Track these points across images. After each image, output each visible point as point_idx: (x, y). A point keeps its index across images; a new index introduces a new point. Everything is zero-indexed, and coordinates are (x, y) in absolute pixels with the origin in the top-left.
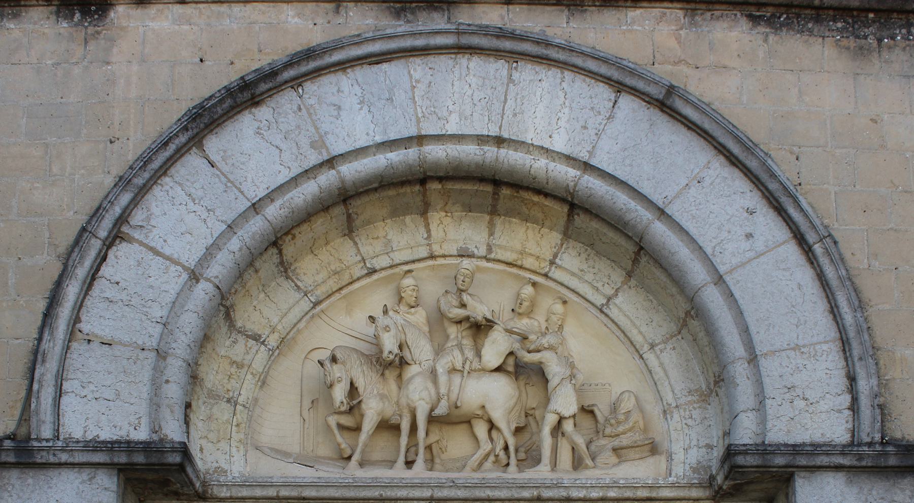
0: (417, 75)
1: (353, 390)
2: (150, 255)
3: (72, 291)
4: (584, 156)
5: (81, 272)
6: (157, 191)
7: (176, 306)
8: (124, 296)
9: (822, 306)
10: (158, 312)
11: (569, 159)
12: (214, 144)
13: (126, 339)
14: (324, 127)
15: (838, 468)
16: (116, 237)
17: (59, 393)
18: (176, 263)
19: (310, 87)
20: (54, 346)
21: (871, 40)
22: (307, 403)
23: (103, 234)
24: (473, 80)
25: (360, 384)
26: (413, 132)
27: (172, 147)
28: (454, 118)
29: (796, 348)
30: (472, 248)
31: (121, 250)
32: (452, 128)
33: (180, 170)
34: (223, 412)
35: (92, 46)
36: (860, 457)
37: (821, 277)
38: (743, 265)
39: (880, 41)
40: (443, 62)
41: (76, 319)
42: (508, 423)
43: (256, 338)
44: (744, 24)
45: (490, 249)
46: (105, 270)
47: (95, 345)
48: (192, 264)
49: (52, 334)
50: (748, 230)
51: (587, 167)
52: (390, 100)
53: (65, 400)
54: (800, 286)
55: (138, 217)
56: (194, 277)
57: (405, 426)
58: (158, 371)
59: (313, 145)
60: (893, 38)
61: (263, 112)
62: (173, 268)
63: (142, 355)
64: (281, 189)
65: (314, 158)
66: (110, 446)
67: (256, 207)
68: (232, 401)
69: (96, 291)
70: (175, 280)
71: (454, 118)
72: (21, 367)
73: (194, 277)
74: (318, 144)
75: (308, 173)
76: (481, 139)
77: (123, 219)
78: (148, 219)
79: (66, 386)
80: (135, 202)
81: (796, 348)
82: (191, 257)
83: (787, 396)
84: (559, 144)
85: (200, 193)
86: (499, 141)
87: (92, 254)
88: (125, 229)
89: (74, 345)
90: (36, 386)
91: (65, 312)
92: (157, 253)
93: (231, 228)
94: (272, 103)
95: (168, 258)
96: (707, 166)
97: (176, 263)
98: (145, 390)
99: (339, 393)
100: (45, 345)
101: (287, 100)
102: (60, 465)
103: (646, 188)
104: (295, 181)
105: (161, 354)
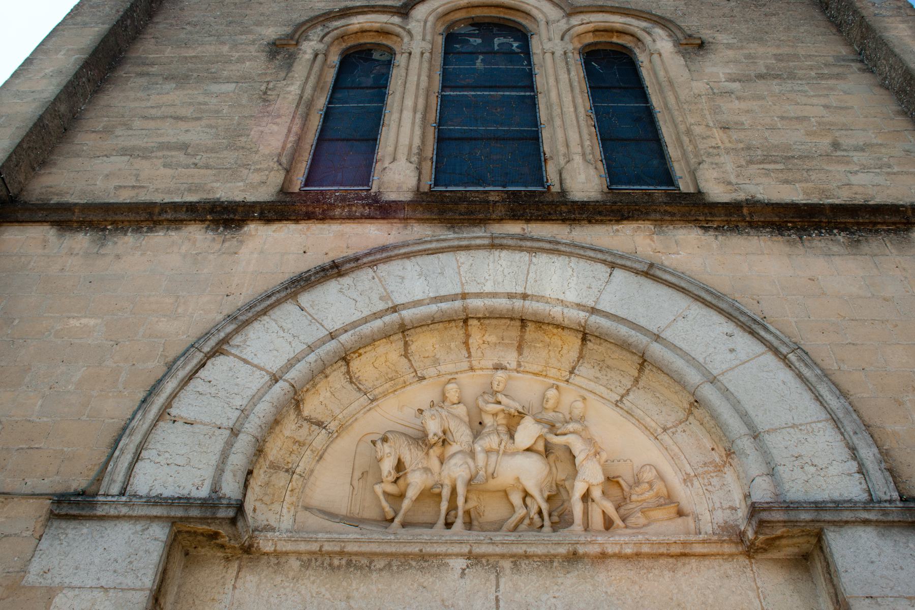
0: (461, 260)
1: (400, 466)
3: (170, 386)
5: (182, 374)
6: (256, 325)
7: (256, 399)
8: (213, 390)
9: (807, 396)
10: (238, 402)
11: (579, 306)
12: (305, 299)
13: (206, 419)
14: (390, 289)
15: (866, 522)
16: (218, 351)
17: (137, 458)
18: (261, 369)
19: (382, 267)
20: (142, 425)
22: (357, 474)
23: (206, 349)
24: (504, 263)
25: (407, 459)
26: (458, 290)
27: (274, 298)
29: (794, 426)
30: (505, 363)
31: (220, 360)
32: (488, 288)
33: (277, 313)
34: (281, 479)
35: (227, 244)
36: (885, 512)
37: (800, 376)
38: (732, 369)
40: (481, 254)
41: (168, 404)
42: (541, 491)
43: (320, 424)
45: (519, 365)
46: (202, 373)
47: (179, 424)
49: (144, 415)
50: (731, 347)
52: (442, 273)
53: (140, 465)
54: (784, 383)
55: (237, 340)
57: (446, 493)
59: (381, 298)
60: (810, 235)
61: (346, 281)
62: (258, 372)
63: (218, 432)
64: (354, 325)
65: (381, 306)
66: (171, 502)
67: (332, 336)
68: (291, 472)
69: (192, 383)
70: (258, 380)
72: (109, 439)
75: (377, 316)
76: (510, 296)
77: (226, 340)
78: (245, 341)
79: (144, 454)
80: (237, 331)
83: (796, 463)
84: (571, 297)
85: (290, 326)
86: (525, 297)
87: (195, 362)
88: (225, 347)
89: (161, 424)
90: (117, 453)
91: (159, 401)
92: (245, 361)
94: (353, 275)
95: (256, 366)
96: (689, 308)
97: (261, 369)
98: (214, 459)
99: (388, 466)
102: (118, 517)
103: (643, 322)
104: (365, 320)
105: (235, 432)
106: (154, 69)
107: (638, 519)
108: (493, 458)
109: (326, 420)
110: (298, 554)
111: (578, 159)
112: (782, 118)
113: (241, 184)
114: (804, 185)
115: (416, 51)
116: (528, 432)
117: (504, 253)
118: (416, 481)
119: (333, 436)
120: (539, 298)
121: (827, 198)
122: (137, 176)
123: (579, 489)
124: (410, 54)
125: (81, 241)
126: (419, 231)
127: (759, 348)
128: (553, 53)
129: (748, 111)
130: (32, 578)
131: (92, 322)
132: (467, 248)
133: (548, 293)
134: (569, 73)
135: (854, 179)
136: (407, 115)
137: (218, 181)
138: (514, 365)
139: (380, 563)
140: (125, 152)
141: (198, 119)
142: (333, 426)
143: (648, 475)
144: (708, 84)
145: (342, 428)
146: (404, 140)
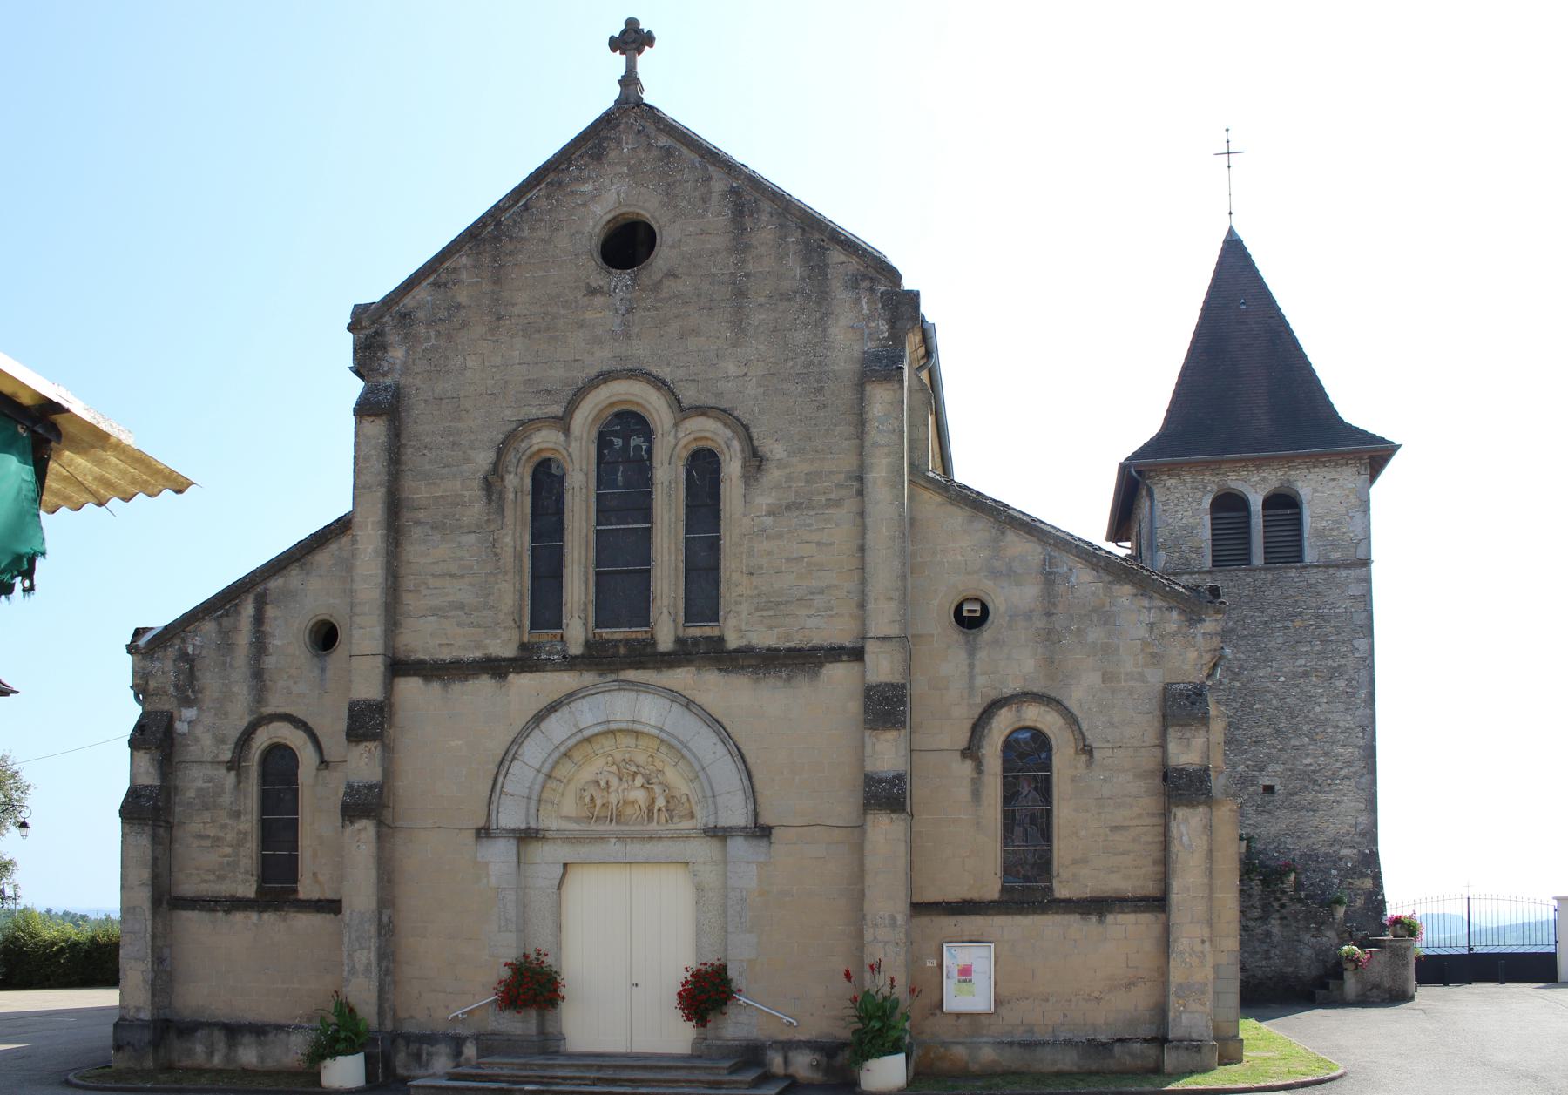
2: (524, 765)
3: (500, 779)
4: (660, 725)
5: (503, 773)
6: (526, 743)
7: (533, 783)
10: (527, 785)
11: (656, 727)
12: (543, 725)
16: (514, 759)
17: (498, 812)
20: (495, 798)
21: (761, 675)
23: (510, 760)
28: (619, 714)
29: (729, 792)
31: (515, 762)
33: (532, 735)
35: (503, 689)
37: (737, 767)
39: (765, 674)
40: (616, 693)
44: (716, 671)
46: (511, 770)
48: (537, 768)
51: (661, 730)
53: (499, 815)
55: (520, 752)
56: (539, 771)
58: (528, 803)
61: (558, 714)
65: (574, 730)
66: (513, 831)
67: (557, 747)
69: (507, 778)
70: (532, 773)
71: (619, 714)
73: (539, 771)
74: (576, 725)
75: (574, 735)
77: (516, 753)
78: (523, 752)
79: (500, 810)
80: (519, 747)
81: (729, 792)
82: (537, 766)
84: (652, 722)
87: (507, 766)
93: (549, 755)
96: (701, 728)
100: (493, 798)
101: (565, 710)
102: (499, 837)
103: (681, 737)
104: (569, 738)
105: (529, 798)
106: (421, 515)
107: (675, 820)
108: (626, 793)
109: (562, 778)
110: (561, 838)
111: (665, 611)
112: (788, 560)
113: (499, 641)
114: (780, 630)
115: (577, 487)
116: (639, 781)
117: (626, 693)
118: (599, 802)
119: (566, 786)
120: (640, 723)
121: (788, 642)
122: (446, 634)
123: (656, 808)
124: (573, 488)
125: (436, 687)
126: (589, 678)
127: (725, 751)
128: (662, 483)
129: (770, 553)
130: (479, 859)
131: (460, 743)
132: (609, 691)
133: (643, 720)
134: (670, 511)
135: (810, 623)
136: (576, 568)
137: (486, 639)
138: (634, 746)
139: (588, 840)
140: (435, 611)
141: (462, 576)
142: (565, 781)
143: (684, 799)
144: (753, 520)
145: (569, 781)
146: (576, 598)
